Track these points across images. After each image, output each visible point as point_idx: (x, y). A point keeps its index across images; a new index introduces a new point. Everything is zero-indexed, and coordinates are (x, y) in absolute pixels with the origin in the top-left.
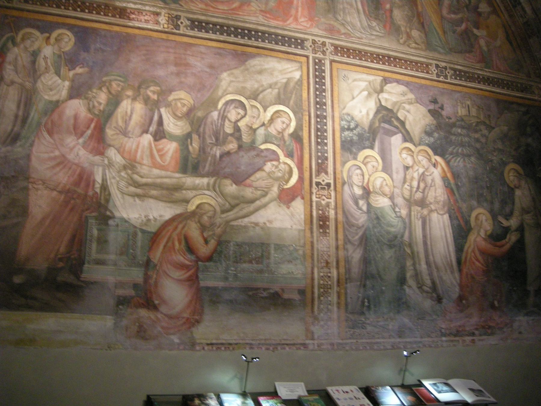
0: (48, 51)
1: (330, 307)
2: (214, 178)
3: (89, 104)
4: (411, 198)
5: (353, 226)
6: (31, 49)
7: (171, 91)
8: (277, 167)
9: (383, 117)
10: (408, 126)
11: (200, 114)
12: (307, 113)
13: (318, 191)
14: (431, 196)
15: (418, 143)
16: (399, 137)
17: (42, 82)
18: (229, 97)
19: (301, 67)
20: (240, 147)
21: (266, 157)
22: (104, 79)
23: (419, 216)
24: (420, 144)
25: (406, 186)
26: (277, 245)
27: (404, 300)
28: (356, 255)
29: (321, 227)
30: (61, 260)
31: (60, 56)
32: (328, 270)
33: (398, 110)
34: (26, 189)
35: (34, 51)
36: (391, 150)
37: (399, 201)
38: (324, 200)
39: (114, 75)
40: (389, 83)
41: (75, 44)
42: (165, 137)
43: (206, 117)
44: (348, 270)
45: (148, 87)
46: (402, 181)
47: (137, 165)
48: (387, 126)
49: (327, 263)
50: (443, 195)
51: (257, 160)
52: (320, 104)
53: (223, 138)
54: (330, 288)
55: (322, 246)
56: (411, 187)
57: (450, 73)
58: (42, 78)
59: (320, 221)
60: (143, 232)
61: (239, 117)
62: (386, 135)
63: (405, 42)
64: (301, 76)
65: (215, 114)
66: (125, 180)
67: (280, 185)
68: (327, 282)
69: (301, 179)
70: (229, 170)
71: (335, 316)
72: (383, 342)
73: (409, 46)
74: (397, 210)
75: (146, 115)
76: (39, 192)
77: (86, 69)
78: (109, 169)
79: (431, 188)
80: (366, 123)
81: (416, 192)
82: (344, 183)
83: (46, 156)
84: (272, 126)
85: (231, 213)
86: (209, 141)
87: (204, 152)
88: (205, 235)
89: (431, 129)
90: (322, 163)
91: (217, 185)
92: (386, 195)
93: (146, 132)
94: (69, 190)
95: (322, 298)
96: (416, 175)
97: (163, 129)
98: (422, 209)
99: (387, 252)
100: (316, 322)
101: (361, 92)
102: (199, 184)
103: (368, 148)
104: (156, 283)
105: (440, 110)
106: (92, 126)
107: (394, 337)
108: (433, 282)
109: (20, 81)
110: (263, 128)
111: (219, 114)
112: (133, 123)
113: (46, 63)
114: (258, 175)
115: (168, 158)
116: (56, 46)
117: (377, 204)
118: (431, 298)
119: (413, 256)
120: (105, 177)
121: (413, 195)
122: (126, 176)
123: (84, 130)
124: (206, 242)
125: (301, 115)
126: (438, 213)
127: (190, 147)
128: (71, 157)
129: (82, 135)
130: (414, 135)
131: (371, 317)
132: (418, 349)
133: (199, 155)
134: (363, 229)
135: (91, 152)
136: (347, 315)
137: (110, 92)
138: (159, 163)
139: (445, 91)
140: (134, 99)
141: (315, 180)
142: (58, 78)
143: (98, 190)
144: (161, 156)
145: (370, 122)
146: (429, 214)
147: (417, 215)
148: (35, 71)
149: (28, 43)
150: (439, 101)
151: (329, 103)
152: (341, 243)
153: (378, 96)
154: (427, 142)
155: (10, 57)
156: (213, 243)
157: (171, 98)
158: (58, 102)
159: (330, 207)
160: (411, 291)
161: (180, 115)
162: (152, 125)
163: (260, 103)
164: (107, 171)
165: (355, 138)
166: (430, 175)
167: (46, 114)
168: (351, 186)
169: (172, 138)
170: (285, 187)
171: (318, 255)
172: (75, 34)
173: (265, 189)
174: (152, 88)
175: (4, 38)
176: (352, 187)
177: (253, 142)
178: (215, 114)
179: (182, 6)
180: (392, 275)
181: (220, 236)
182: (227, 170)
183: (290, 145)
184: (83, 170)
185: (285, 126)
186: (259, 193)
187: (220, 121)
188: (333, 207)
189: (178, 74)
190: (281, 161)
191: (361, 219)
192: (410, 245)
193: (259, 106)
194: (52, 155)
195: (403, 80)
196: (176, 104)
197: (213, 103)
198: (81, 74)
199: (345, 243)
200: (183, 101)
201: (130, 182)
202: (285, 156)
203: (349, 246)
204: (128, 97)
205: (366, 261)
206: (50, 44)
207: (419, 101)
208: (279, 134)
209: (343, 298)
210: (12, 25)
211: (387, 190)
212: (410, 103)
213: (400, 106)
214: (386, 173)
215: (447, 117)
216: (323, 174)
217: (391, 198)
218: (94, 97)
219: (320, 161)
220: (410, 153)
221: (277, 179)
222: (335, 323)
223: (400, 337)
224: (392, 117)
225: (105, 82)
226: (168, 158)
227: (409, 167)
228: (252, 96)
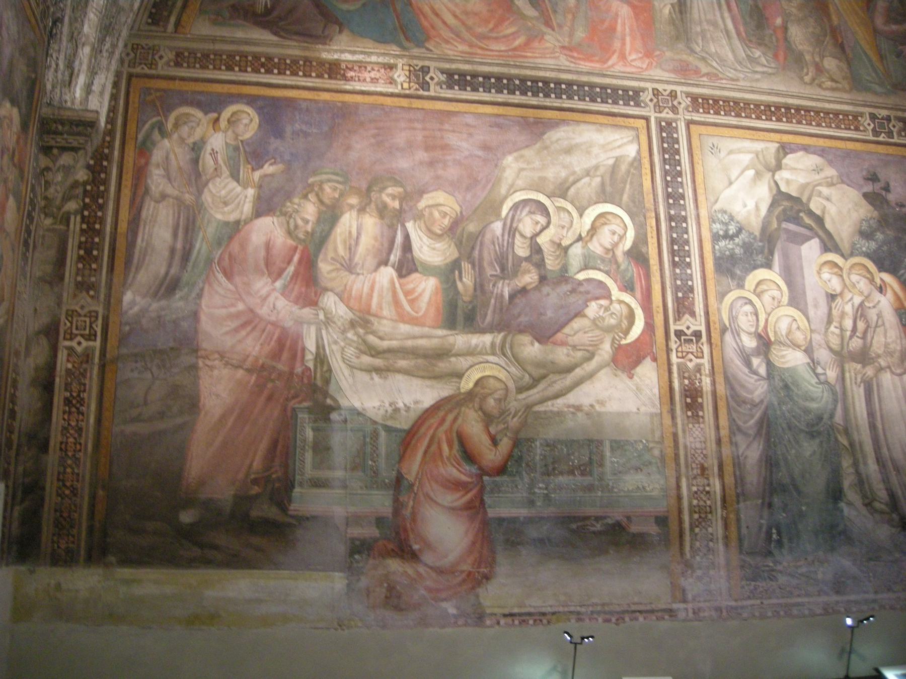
0: (217, 141)
1: (711, 544)
2: (502, 334)
3: (288, 223)
4: (842, 348)
5: (744, 402)
6: (191, 141)
7: (421, 192)
8: (607, 309)
9: (784, 211)
10: (828, 225)
11: (472, 227)
12: (653, 215)
13: (681, 345)
14: (878, 343)
15: (849, 252)
16: (815, 243)
17: (211, 192)
18: (519, 196)
19: (638, 137)
20: (543, 279)
21: (588, 293)
22: (311, 180)
23: (859, 380)
24: (852, 255)
25: (832, 328)
26: (615, 441)
27: (841, 527)
28: (753, 453)
29: (688, 407)
30: (255, 482)
31: (236, 149)
32: (706, 482)
33: (809, 199)
34: (194, 367)
35: (195, 144)
36: (802, 268)
37: (823, 355)
38: (691, 360)
39: (326, 173)
40: (791, 153)
41: (260, 125)
42: (416, 270)
43: (481, 233)
44: (740, 480)
45: (385, 188)
46: (825, 320)
47: (372, 319)
48: (792, 227)
49: (703, 469)
50: (899, 341)
51: (572, 299)
52: (674, 198)
53: (513, 265)
54: (711, 512)
55: (692, 439)
56: (842, 330)
57: (897, 127)
58: (210, 185)
59: (687, 396)
60: (389, 429)
61: (538, 228)
62: (792, 242)
63: (813, 80)
64: (639, 152)
65: (497, 227)
66: (355, 345)
67: (614, 338)
68: (705, 502)
69: (649, 326)
70: (527, 319)
71: (721, 559)
72: (809, 603)
73: (820, 86)
74: (819, 370)
75: (382, 236)
76: (216, 372)
77: (280, 167)
78: (327, 328)
79: (878, 329)
80: (755, 224)
81: (851, 337)
82: (724, 330)
83: (224, 312)
84: (595, 238)
85: (531, 392)
86: (489, 272)
87: (483, 291)
88: (493, 430)
89: (870, 227)
90: (683, 297)
91: (507, 346)
92: (799, 347)
93: (385, 263)
94: (263, 366)
95: (697, 530)
96: (848, 308)
97: (412, 256)
98: (864, 367)
99: (805, 444)
100: (689, 572)
101: (743, 172)
102: (477, 346)
103: (762, 266)
104: (414, 514)
105: (884, 193)
106: (296, 258)
107: (827, 594)
108: (892, 495)
109: (176, 193)
110: (580, 244)
111: (504, 225)
112: (361, 249)
113: (216, 161)
114: (577, 324)
115: (423, 303)
116: (230, 133)
117: (783, 363)
118: (890, 522)
119: (853, 448)
120: (320, 342)
121: (845, 344)
122: (355, 338)
123: (284, 266)
124: (494, 441)
125: (642, 219)
126: (892, 373)
127: (459, 285)
128: (263, 311)
129: (280, 275)
130: (842, 239)
131: (785, 559)
132: (871, 614)
133: (475, 296)
134: (763, 407)
135: (296, 302)
136: (743, 557)
137: (321, 202)
138: (408, 313)
139: (890, 158)
140: (362, 210)
141: (673, 328)
142: (235, 184)
143: (311, 365)
144: (412, 302)
145: (763, 223)
146: (876, 375)
147: (856, 379)
148: (198, 175)
149: (185, 130)
150: (880, 176)
151: (689, 193)
152: (724, 432)
153: (773, 176)
154: (864, 249)
155: (157, 156)
156: (505, 444)
157: (422, 204)
158: (238, 222)
159: (702, 371)
160: (853, 512)
161: (439, 232)
162: (394, 251)
163: (572, 203)
164: (324, 332)
165: (738, 251)
166: (874, 307)
167: (219, 244)
168: (737, 334)
169: (429, 270)
170: (623, 342)
171: (686, 456)
172: (259, 110)
173: (590, 348)
174: (390, 190)
175: (147, 126)
176: (739, 335)
177: (565, 268)
178: (497, 227)
179: (431, 51)
180: (817, 485)
181: (517, 432)
182: (523, 319)
183: (627, 270)
184: (284, 332)
185: (616, 238)
186: (579, 354)
187: (506, 237)
188: (707, 372)
189: (431, 164)
190: (613, 298)
191: (757, 389)
192: (847, 432)
193: (570, 207)
194: (233, 310)
195: (815, 146)
196: (431, 214)
197: (492, 208)
198: (272, 175)
199: (732, 433)
200: (441, 208)
201: (362, 348)
202: (620, 290)
203: (739, 438)
204: (352, 207)
205: (770, 462)
206: (220, 129)
207: (845, 179)
208: (606, 254)
209: (733, 528)
210: (158, 104)
211: (799, 337)
212: (831, 185)
213: (812, 191)
214: (798, 309)
215: (897, 204)
216: (687, 316)
217: (809, 351)
218: (297, 211)
219: (680, 295)
220: (836, 270)
221: (609, 329)
222: (723, 573)
223: (837, 592)
224: (800, 211)
225: (311, 186)
226: (423, 303)
227: (836, 295)
228: (557, 192)
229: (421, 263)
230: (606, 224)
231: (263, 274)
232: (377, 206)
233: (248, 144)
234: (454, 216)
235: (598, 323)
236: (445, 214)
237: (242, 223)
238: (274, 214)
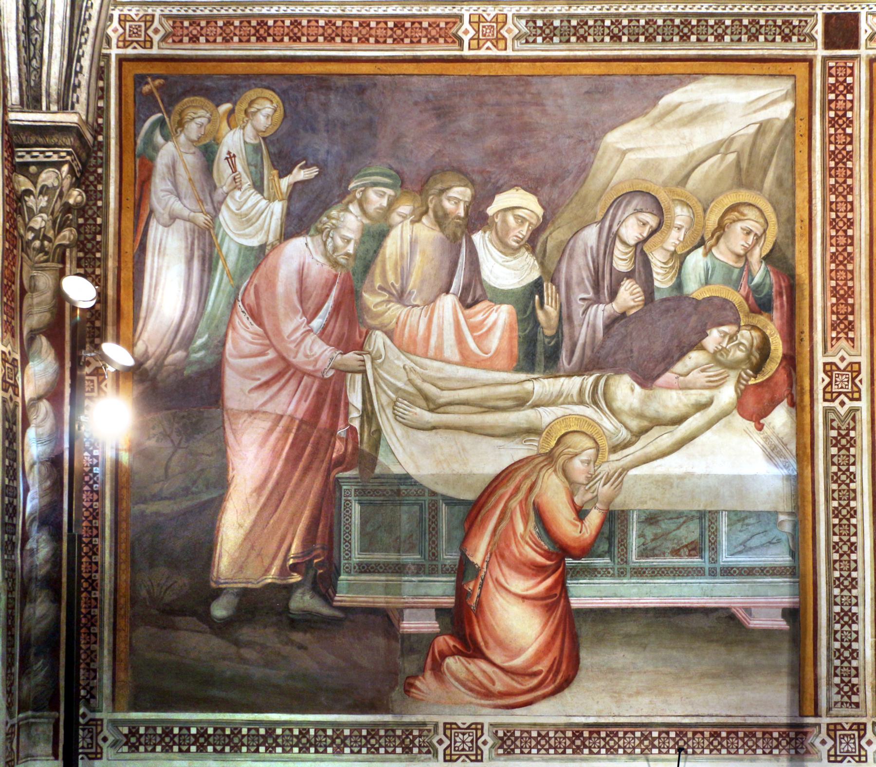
3: (325, 244)
26: (736, 512)
30: (294, 568)
31: (257, 149)
41: (285, 116)
58: (228, 200)
60: (452, 502)
64: (794, 112)
77: (313, 172)
84: (722, 240)
85: (631, 449)
88: (578, 500)
104: (479, 604)
124: (581, 514)
127: (540, 313)
128: (299, 360)
137: (364, 212)
142: (259, 196)
143: (356, 424)
144: (478, 340)
156: (594, 518)
157: (491, 211)
158: (262, 247)
169: (500, 297)
172: (283, 95)
181: (610, 502)
196: (504, 221)
200: (519, 212)
226: (494, 342)
229: (490, 286)
230: (739, 220)
231: (296, 312)
232: (436, 216)
233: (272, 142)
234: (534, 221)
235: (719, 357)
236: (522, 220)
237: (269, 248)
238: (307, 233)
